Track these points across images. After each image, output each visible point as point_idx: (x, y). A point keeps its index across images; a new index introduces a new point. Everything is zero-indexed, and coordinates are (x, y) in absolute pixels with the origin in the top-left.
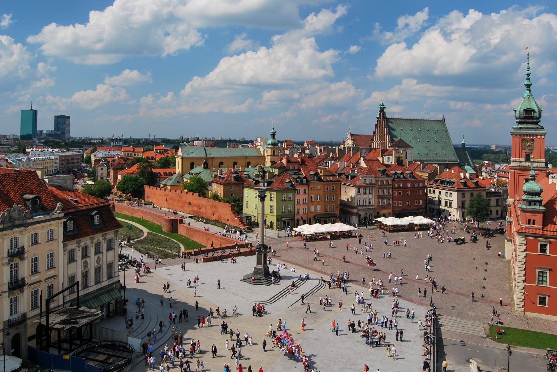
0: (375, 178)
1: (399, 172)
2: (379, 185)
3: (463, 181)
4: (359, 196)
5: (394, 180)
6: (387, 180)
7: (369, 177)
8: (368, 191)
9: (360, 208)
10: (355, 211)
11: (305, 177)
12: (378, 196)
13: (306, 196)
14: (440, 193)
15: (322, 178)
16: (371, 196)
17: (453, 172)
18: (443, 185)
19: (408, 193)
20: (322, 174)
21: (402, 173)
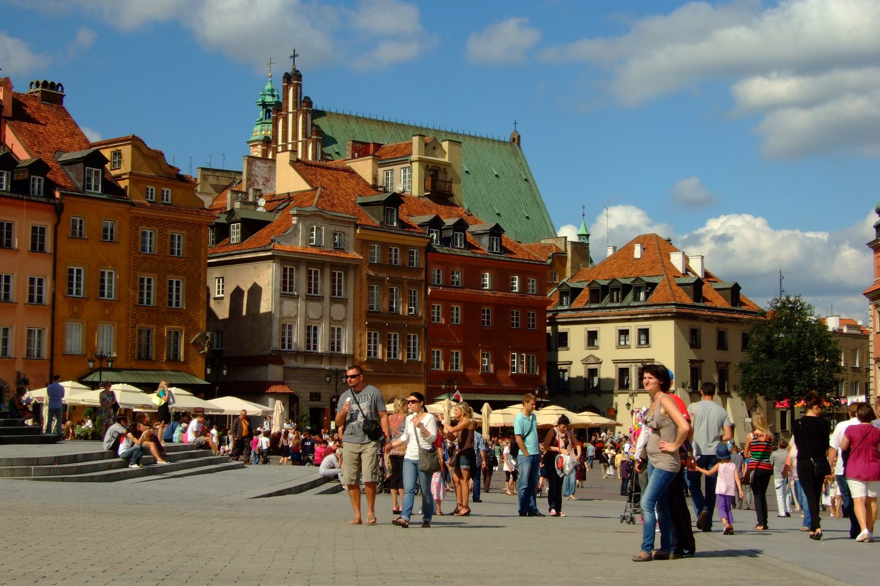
0: (357, 226)
1: (449, 222)
2: (372, 266)
3: (691, 279)
4: (289, 306)
5: (429, 249)
6: (404, 247)
7: (332, 220)
8: (325, 288)
9: (292, 363)
10: (274, 372)
11: (39, 167)
12: (371, 313)
13: (42, 267)
14: (592, 337)
15: (123, 184)
16: (338, 310)
17: (637, 252)
18: (606, 302)
19: (487, 317)
20: (126, 167)
21: (461, 226)
